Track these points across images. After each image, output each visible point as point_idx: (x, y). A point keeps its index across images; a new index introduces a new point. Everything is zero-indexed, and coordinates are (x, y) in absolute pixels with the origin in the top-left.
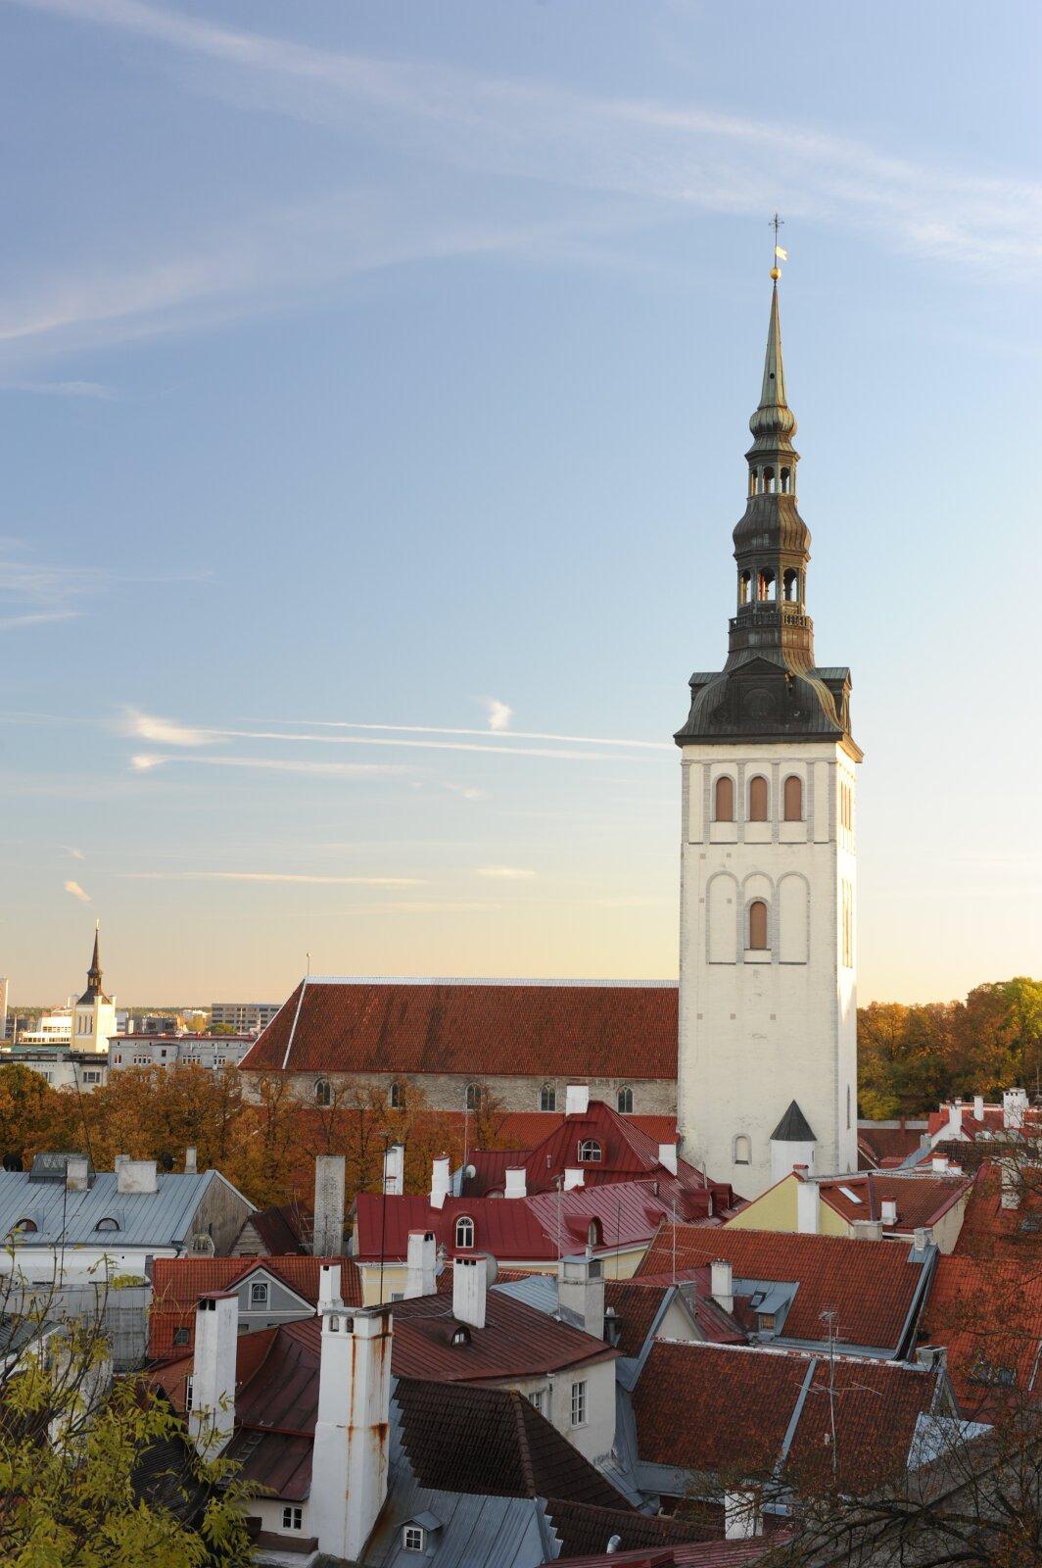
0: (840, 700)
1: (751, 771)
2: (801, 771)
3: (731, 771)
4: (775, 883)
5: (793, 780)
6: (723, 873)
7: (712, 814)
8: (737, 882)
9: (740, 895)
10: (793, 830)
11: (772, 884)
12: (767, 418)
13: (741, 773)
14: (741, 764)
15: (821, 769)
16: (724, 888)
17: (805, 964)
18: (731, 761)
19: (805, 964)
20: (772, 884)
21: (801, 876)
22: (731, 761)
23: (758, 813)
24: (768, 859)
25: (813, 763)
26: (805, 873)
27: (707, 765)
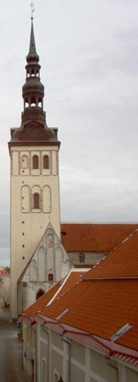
0: (56, 134)
1: (33, 154)
2: (48, 153)
3: (27, 154)
4: (41, 187)
5: (46, 157)
9: (31, 191)
12: (33, 55)
13: (30, 155)
15: (54, 154)
16: (26, 190)
21: (49, 186)
23: (36, 166)
24: (42, 181)
26: (51, 186)
27: (19, 152)
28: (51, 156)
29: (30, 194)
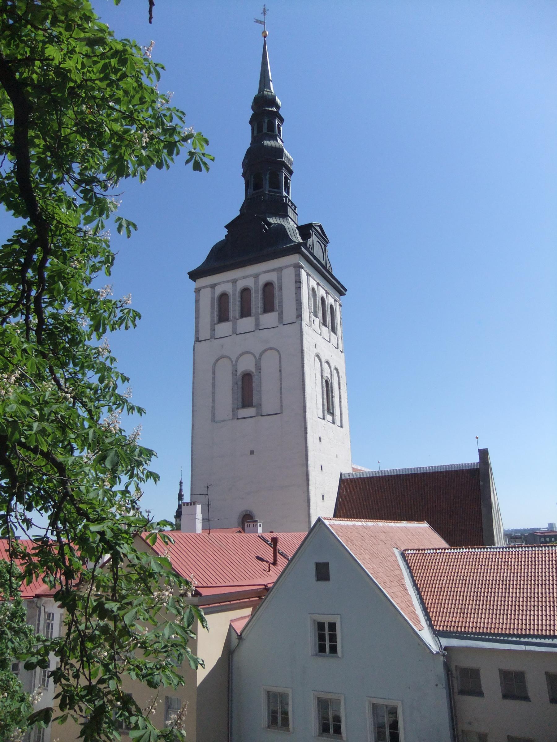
1: (241, 285)
6: (222, 357)
7: (216, 319)
8: (232, 362)
9: (235, 371)
10: (269, 319)
11: (255, 357)
14: (234, 282)
15: (288, 275)
17: (279, 413)
18: (228, 282)
19: (279, 413)
20: (255, 357)
22: (228, 282)
23: (245, 312)
25: (282, 270)
28: (280, 279)
29: (234, 373)
